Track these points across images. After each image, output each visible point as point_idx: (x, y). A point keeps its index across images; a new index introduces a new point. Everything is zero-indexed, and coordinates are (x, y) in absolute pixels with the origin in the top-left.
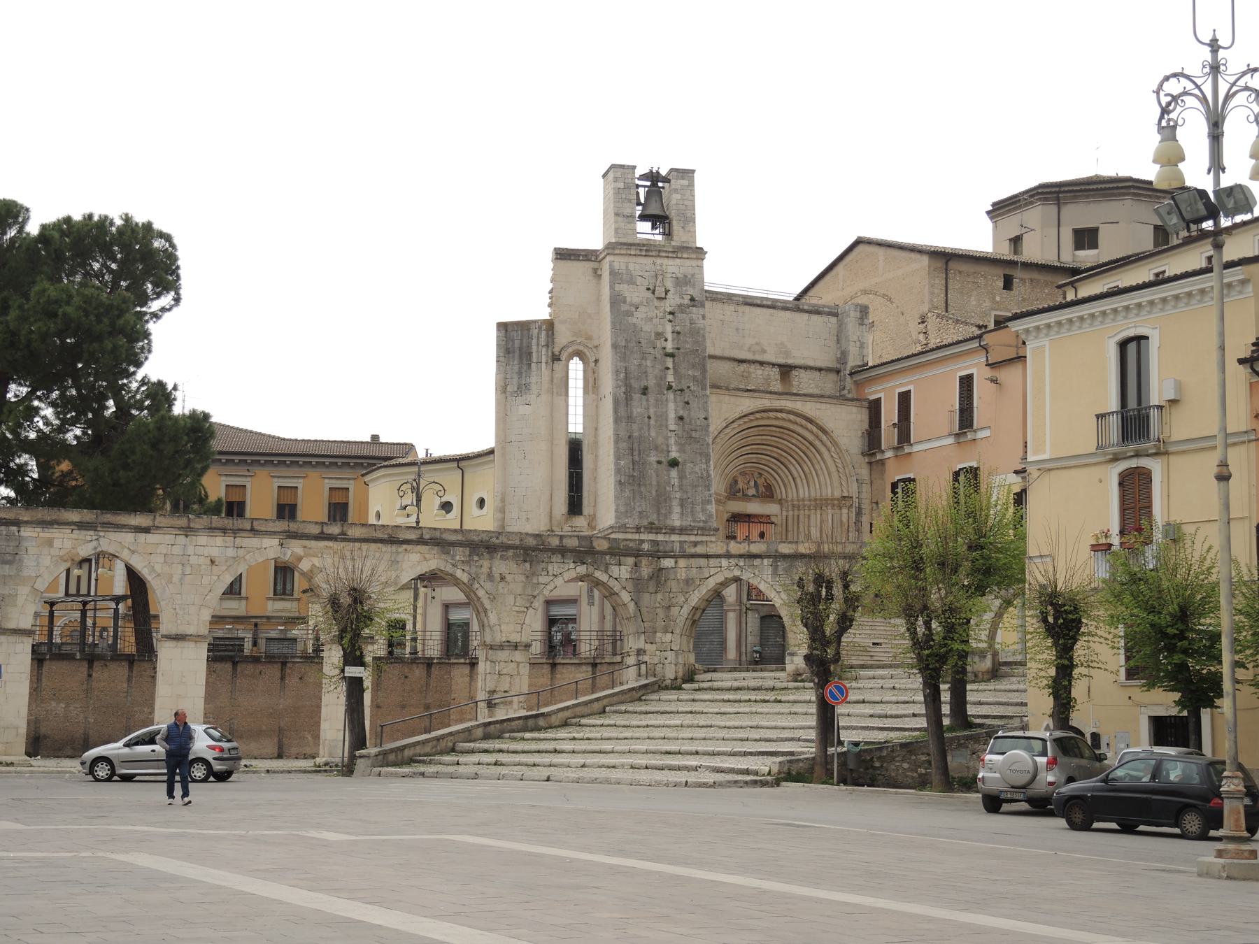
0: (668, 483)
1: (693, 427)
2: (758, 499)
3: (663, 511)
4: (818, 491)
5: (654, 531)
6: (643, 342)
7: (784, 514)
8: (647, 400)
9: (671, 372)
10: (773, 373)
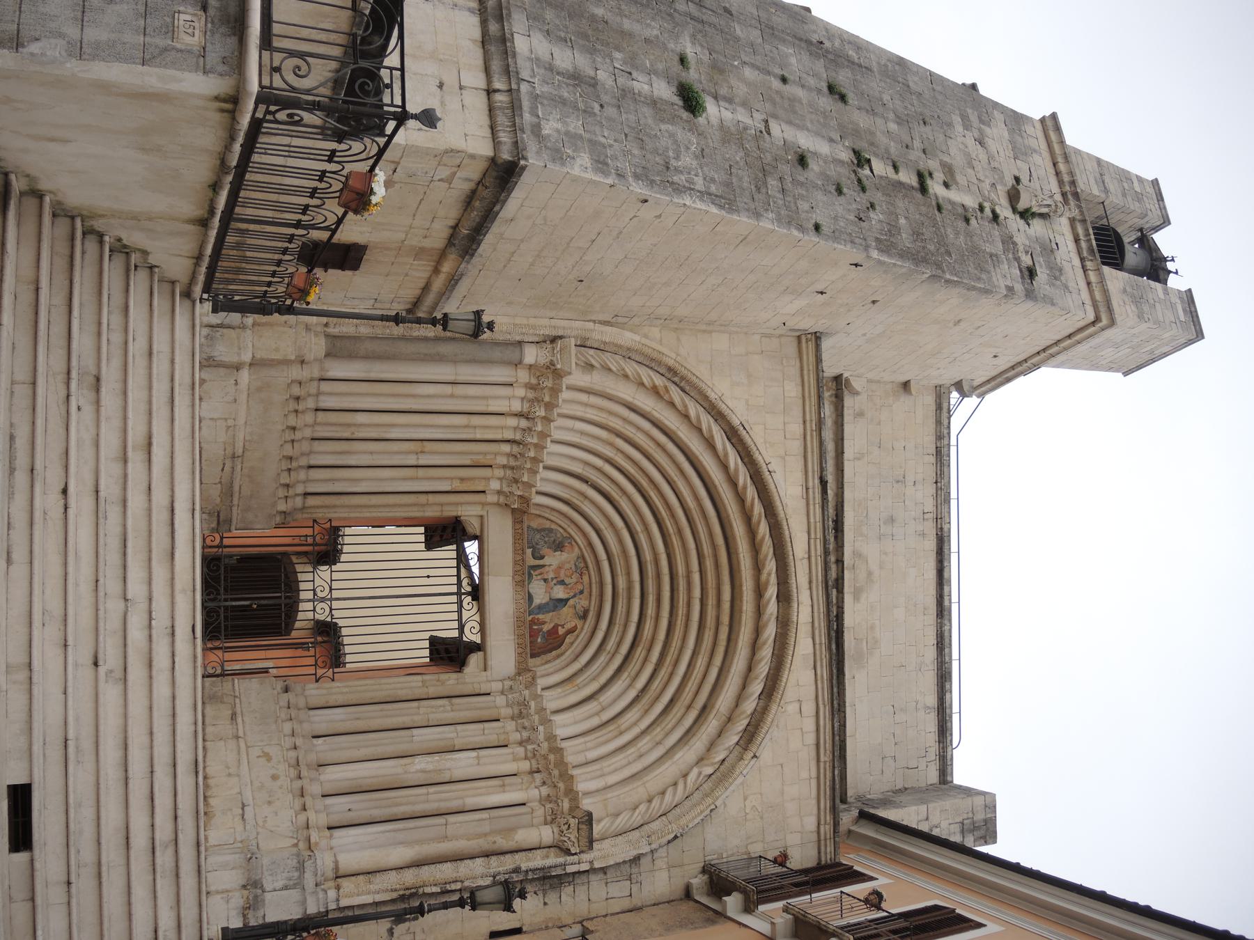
0: (632, 61)
7: (496, 686)
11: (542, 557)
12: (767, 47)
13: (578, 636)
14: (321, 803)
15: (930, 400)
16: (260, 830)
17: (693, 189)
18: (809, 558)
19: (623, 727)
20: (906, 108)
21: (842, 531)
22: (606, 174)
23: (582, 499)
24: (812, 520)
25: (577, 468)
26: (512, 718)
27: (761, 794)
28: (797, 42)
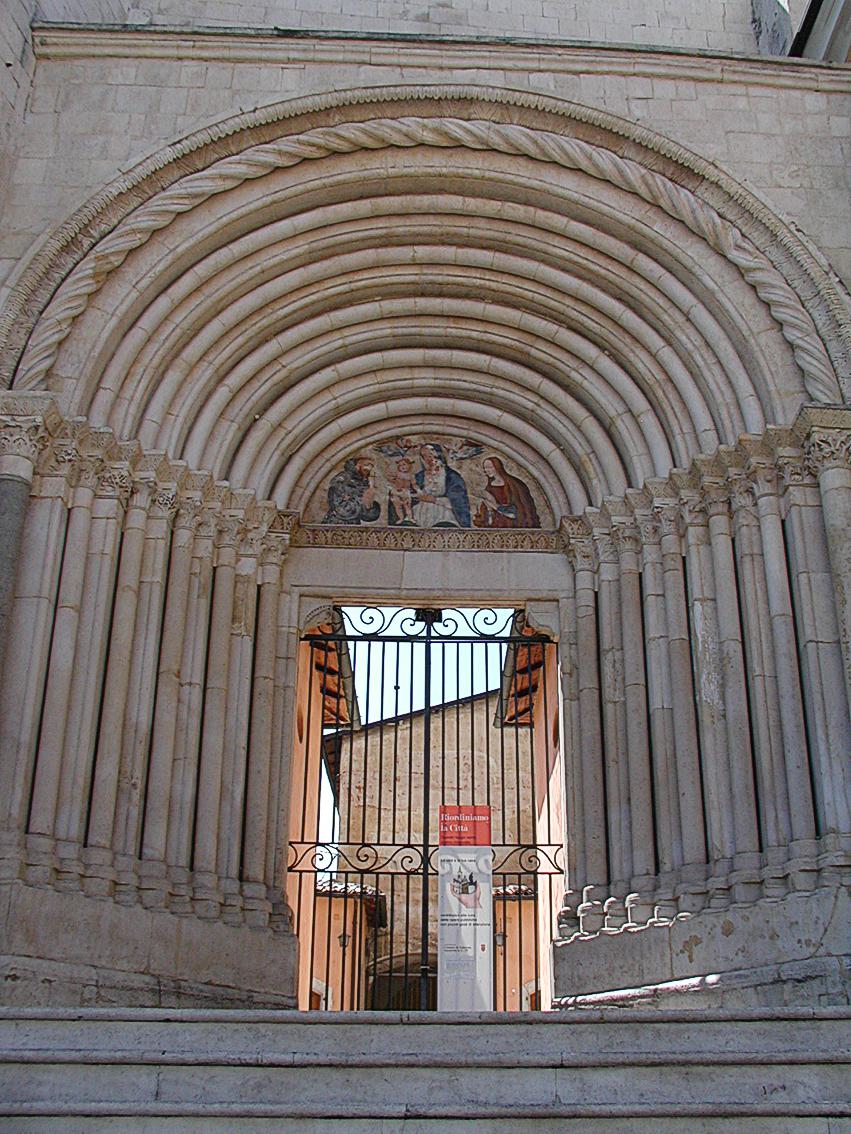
2: (451, 537)
11: (377, 506)
14: (774, 855)
16: (822, 951)
19: (660, 376)
23: (282, 433)
24: (340, 57)
25: (229, 433)
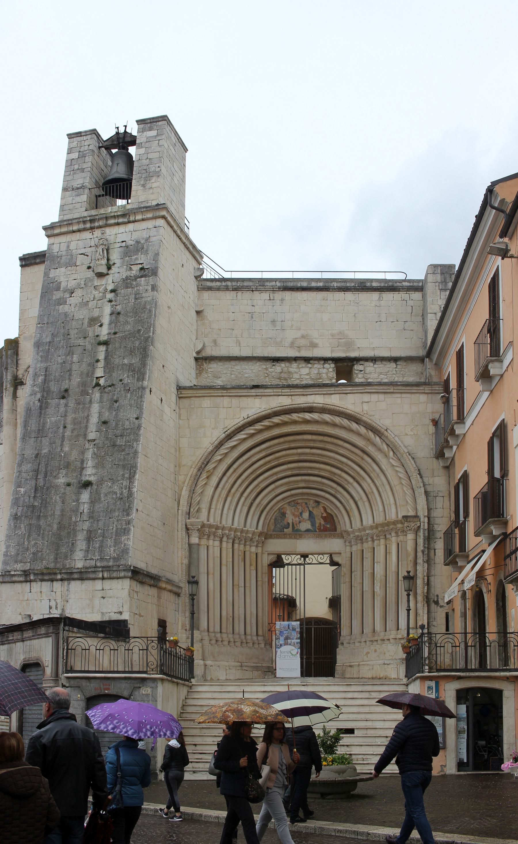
0: (75, 510)
1: (118, 432)
3: (63, 550)
4: (382, 514)
5: (46, 577)
6: (73, 332)
7: (348, 549)
8: (66, 405)
9: (101, 364)
10: (325, 371)
11: (288, 524)
12: (50, 435)
13: (328, 506)
15: (206, 294)
17: (129, 487)
18: (291, 395)
19: (370, 491)
20: (63, 347)
21: (279, 357)
22: (129, 530)
24: (272, 394)
25: (245, 509)
26: (362, 543)
27: (406, 426)
28: (42, 416)
